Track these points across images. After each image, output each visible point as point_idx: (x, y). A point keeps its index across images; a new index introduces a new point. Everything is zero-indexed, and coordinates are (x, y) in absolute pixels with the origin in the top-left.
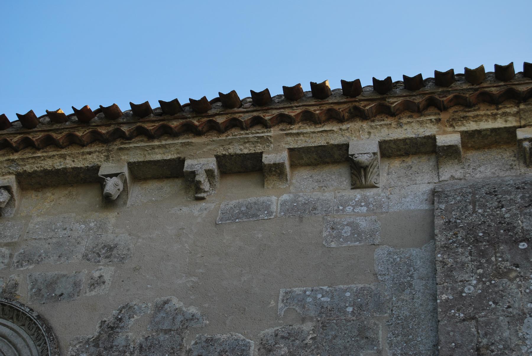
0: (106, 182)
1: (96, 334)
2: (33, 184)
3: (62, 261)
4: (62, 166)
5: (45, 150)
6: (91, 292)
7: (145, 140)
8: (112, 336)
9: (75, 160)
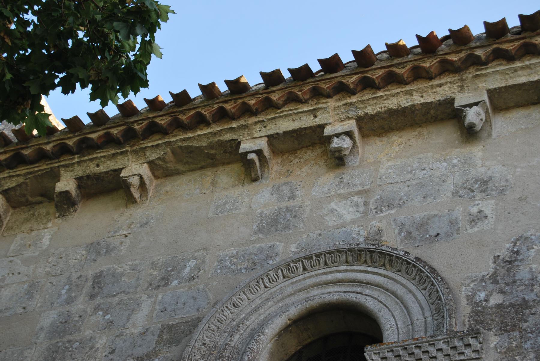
0: (465, 112)
1: (492, 271)
2: (375, 129)
3: (428, 202)
4: (410, 104)
5: (386, 88)
6: (474, 229)
7: (504, 63)
8: (512, 270)
9: (424, 95)
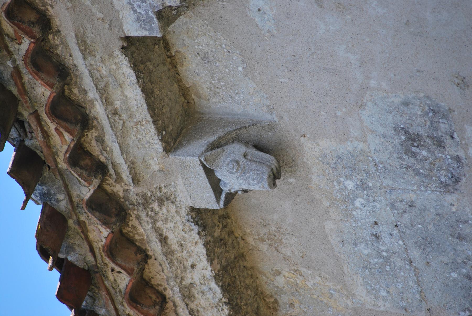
7: (95, 134)
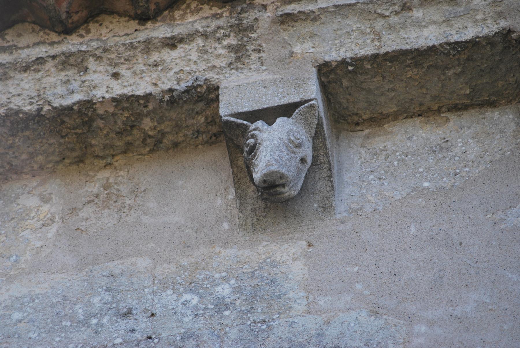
4: (77, 97)
9: (122, 70)
